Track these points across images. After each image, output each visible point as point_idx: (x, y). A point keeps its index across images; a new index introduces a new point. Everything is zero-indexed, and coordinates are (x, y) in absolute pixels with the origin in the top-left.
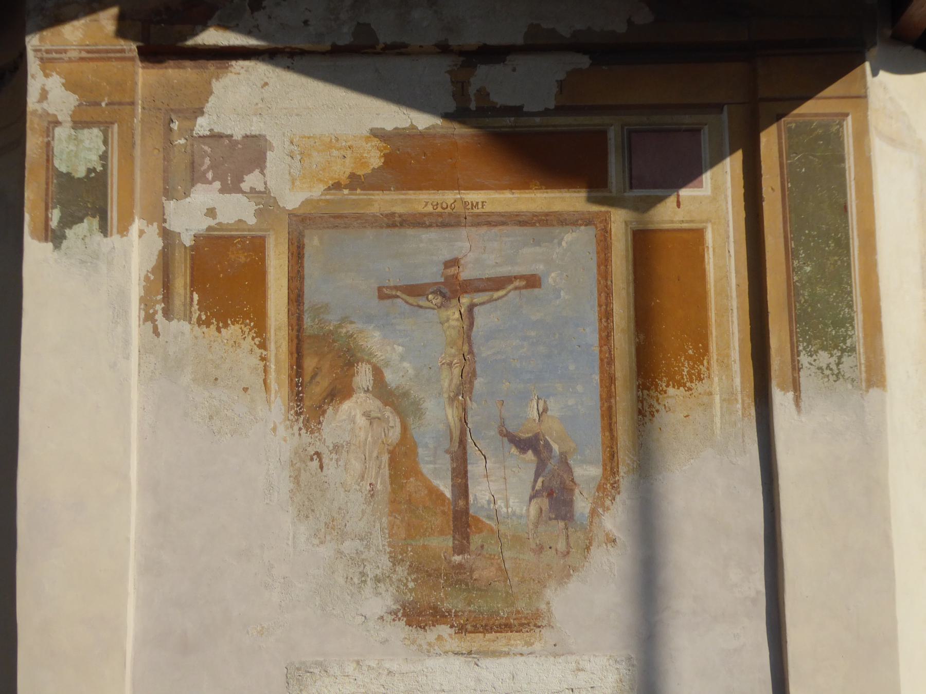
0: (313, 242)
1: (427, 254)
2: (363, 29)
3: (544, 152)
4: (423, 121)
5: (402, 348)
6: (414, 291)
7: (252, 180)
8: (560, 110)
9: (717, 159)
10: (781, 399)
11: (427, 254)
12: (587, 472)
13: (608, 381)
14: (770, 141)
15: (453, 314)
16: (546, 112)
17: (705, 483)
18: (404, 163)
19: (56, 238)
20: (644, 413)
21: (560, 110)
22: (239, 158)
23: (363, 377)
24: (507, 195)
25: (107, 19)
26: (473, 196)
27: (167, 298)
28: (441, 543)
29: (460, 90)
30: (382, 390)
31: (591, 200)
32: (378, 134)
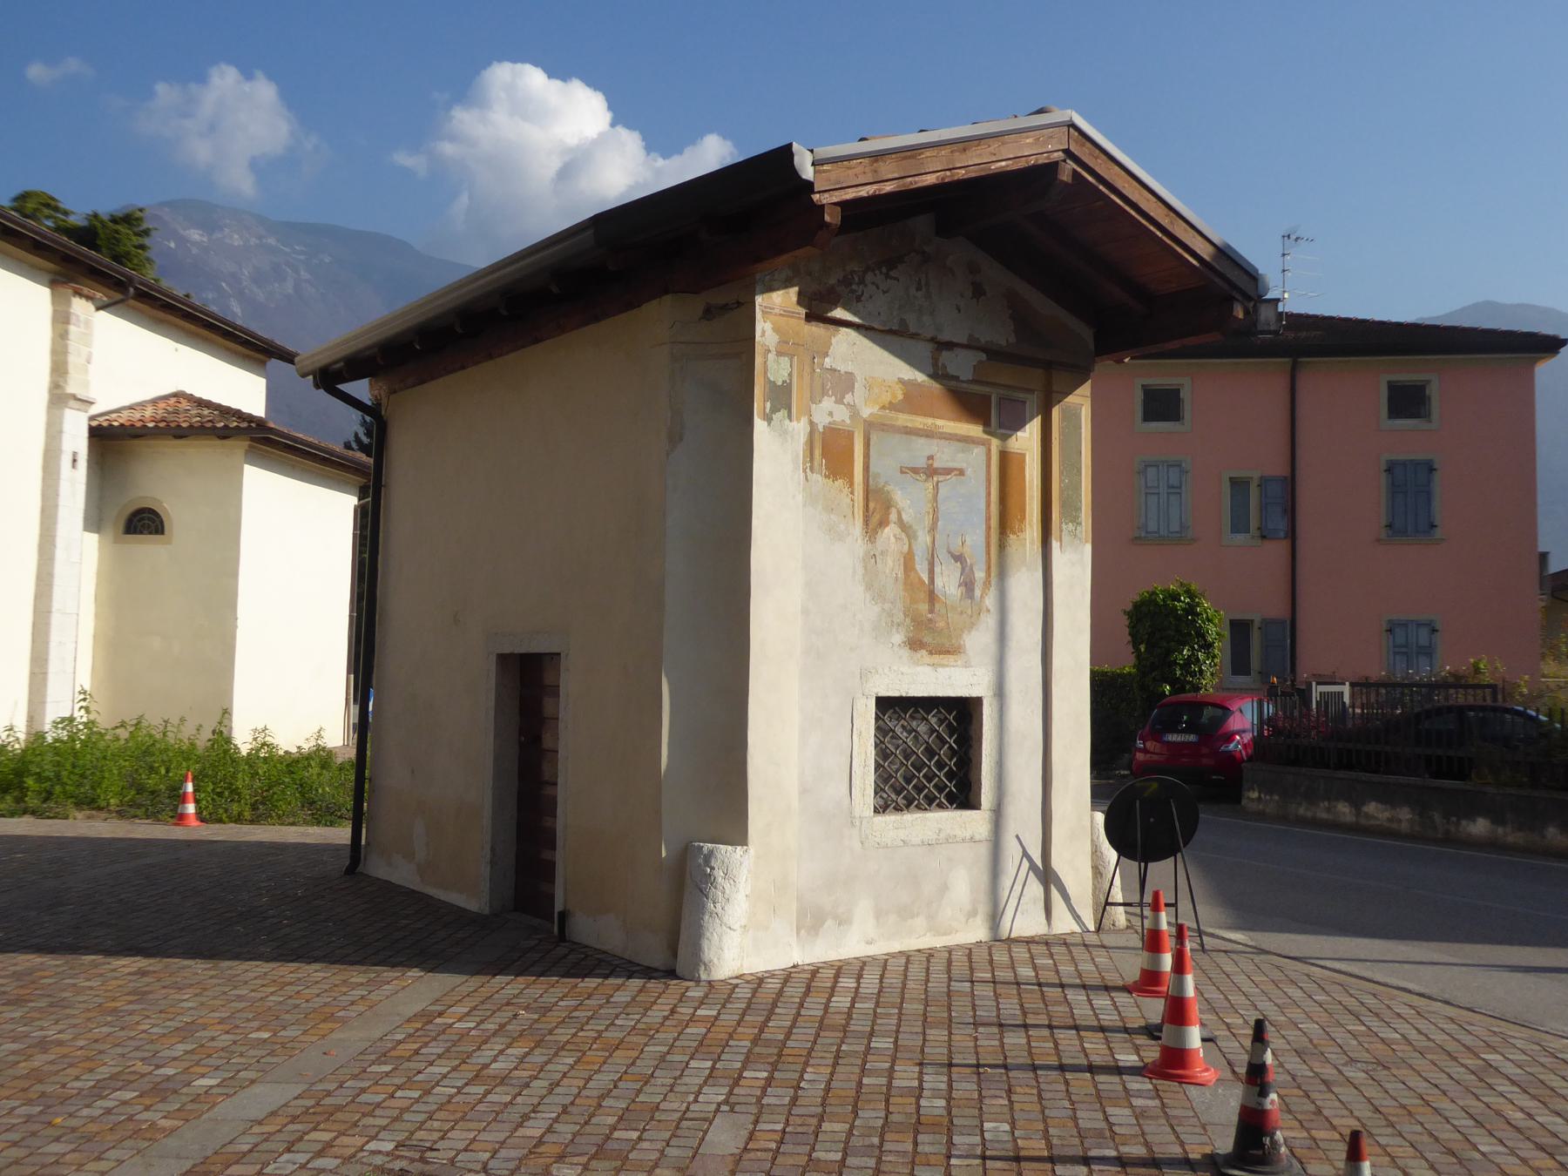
0: (874, 438)
1: (921, 450)
2: (903, 322)
3: (972, 405)
4: (920, 377)
5: (909, 500)
6: (915, 471)
7: (848, 398)
8: (974, 381)
9: (1031, 419)
10: (1055, 545)
11: (921, 450)
12: (980, 575)
13: (989, 528)
14: (1056, 412)
15: (930, 485)
16: (968, 382)
17: (1024, 585)
18: (911, 401)
19: (768, 419)
20: (1002, 546)
21: (974, 381)
22: (843, 384)
23: (893, 516)
24: (952, 424)
25: (793, 292)
26: (940, 422)
27: (812, 460)
28: (924, 607)
29: (935, 365)
30: (902, 525)
31: (985, 432)
32: (901, 381)
